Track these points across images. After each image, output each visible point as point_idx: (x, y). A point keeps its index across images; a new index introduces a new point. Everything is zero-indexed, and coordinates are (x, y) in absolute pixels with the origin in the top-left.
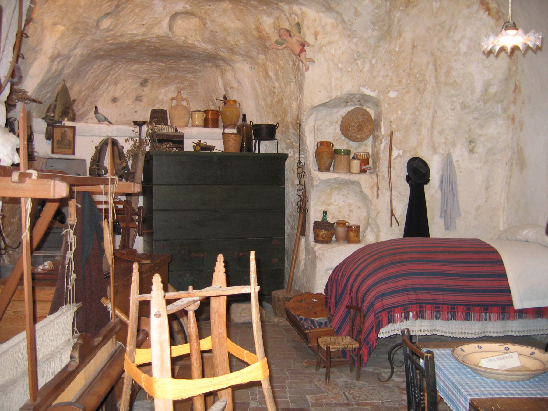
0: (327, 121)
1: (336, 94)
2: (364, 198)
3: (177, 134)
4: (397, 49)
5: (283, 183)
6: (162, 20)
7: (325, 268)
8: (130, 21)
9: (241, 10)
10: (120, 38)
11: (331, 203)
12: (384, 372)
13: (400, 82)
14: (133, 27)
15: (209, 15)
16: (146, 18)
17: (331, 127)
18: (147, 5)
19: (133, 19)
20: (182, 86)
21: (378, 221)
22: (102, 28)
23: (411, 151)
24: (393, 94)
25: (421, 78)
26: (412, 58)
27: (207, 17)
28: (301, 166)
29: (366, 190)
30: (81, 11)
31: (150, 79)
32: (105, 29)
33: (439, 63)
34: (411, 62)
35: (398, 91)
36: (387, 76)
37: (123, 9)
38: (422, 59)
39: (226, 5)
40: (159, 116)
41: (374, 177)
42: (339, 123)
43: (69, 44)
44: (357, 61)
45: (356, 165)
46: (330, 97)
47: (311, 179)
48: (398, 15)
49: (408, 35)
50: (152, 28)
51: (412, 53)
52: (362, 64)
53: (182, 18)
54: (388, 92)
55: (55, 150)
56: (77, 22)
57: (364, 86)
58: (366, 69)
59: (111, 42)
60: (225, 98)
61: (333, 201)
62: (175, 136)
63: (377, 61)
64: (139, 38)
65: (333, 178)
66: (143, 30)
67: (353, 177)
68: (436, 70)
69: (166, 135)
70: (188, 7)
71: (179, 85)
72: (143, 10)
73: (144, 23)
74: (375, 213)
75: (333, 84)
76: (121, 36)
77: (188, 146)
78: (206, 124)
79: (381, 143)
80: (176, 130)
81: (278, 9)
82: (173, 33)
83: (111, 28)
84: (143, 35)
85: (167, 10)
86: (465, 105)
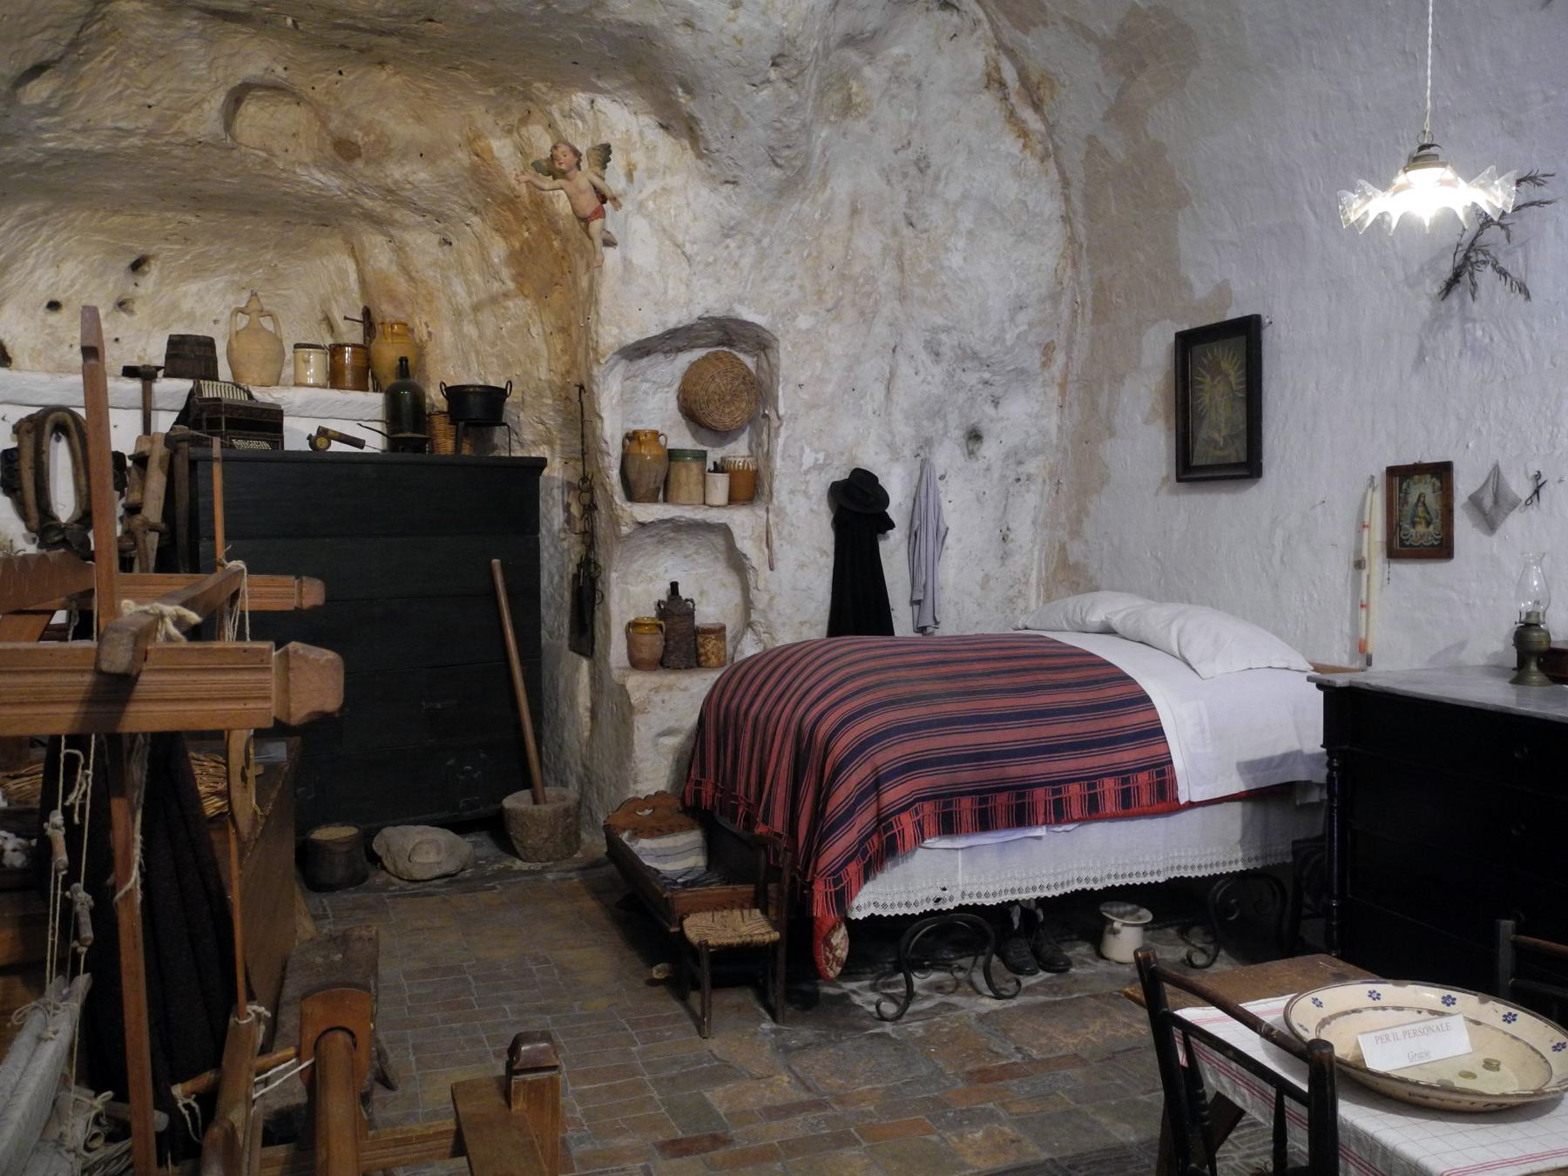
1: (676, 318)
2: (737, 563)
3: (251, 404)
4: (817, 216)
5: (535, 528)
6: (203, 100)
7: (655, 731)
8: (111, 93)
9: (426, 91)
11: (657, 575)
12: (854, 992)
13: (820, 293)
14: (120, 108)
15: (337, 99)
16: (158, 87)
17: (659, 395)
18: (162, 53)
19: (119, 88)
20: (246, 279)
21: (772, 616)
22: (25, 102)
23: (842, 454)
24: (804, 322)
25: (867, 288)
26: (850, 240)
27: (332, 103)
28: (586, 488)
29: (745, 545)
31: (154, 257)
32: (32, 107)
33: (909, 252)
34: (847, 248)
35: (816, 314)
36: (792, 278)
37: (89, 56)
38: (870, 243)
39: (384, 75)
41: (762, 513)
42: (676, 386)
44: (728, 241)
45: (720, 486)
46: (663, 324)
47: (615, 521)
48: (823, 134)
49: (841, 187)
50: (176, 117)
51: (851, 228)
52: (739, 247)
53: (259, 98)
54: (795, 318)
57: (741, 301)
58: (746, 262)
60: (367, 313)
61: (661, 570)
62: (246, 408)
63: (772, 242)
64: (136, 141)
65: (667, 516)
66: (148, 121)
67: (714, 516)
68: (901, 269)
70: (279, 70)
71: (236, 278)
72: (149, 64)
73: (151, 101)
74: (766, 597)
75: (671, 293)
77: (297, 435)
78: (335, 379)
79: (777, 435)
80: (250, 397)
81: (527, 97)
82: (233, 138)
83: (53, 105)
84: (149, 134)
85: (221, 73)
86: (964, 351)
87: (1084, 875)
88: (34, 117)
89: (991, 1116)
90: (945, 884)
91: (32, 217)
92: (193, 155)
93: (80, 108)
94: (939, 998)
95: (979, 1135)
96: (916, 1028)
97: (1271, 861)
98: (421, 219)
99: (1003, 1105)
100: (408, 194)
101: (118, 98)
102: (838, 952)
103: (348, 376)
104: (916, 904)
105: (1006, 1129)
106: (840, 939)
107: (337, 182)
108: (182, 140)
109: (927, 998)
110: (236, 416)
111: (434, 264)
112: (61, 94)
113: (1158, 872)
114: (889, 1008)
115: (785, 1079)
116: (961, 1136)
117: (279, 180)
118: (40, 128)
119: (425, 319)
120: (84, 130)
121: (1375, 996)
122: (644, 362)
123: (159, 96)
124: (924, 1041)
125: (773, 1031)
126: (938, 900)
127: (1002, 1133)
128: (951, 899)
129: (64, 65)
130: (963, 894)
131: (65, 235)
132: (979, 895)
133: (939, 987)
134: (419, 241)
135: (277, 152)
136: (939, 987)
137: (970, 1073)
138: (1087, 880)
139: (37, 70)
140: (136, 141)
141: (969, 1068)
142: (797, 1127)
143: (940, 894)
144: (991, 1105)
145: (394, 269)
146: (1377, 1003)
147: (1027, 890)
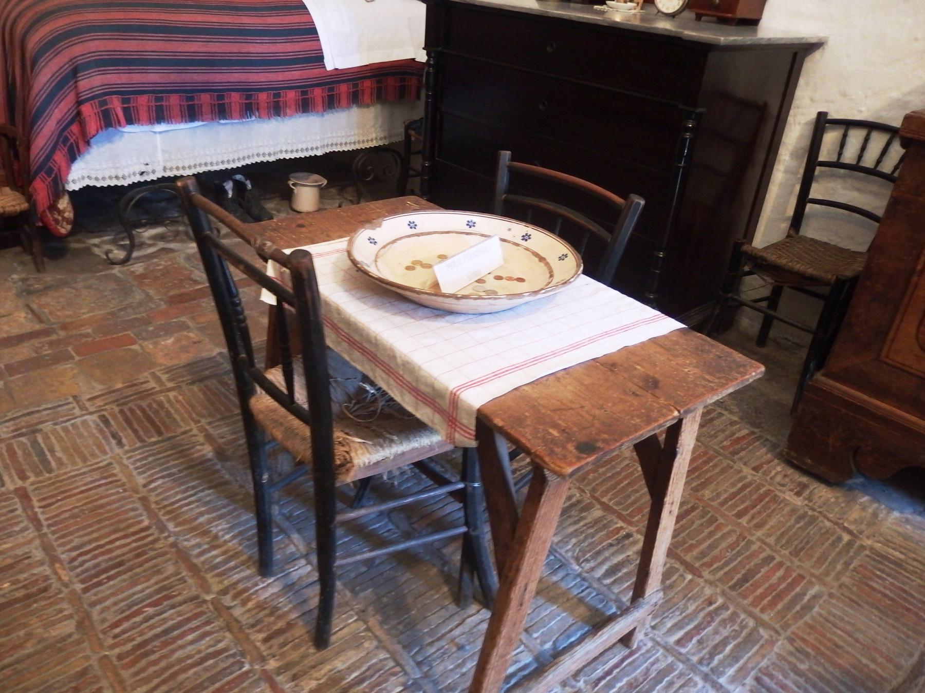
12: (95, 245)
87: (261, 152)
89: (183, 327)
90: (148, 161)
94: (161, 245)
95: (170, 341)
96: (138, 268)
97: (394, 140)
99: (193, 318)
102: (66, 215)
104: (124, 178)
105: (191, 335)
106: (64, 203)
109: (150, 245)
113: (317, 148)
114: (119, 254)
115: (22, 316)
116: (156, 344)
121: (412, 225)
124: (143, 276)
125: (23, 280)
126: (142, 173)
127: (188, 338)
128: (154, 172)
130: (165, 169)
132: (178, 168)
133: (161, 237)
136: (161, 237)
137: (172, 297)
138: (264, 155)
141: (172, 293)
142: (24, 351)
143: (144, 169)
144: (183, 319)
146: (413, 231)
147: (217, 164)
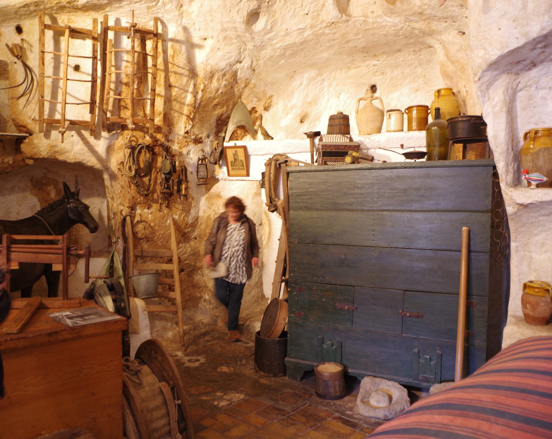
0: (543, 88)
8: (290, 14)
10: (287, 39)
14: (296, 20)
19: (292, 11)
22: (256, 30)
30: (219, 15)
32: (260, 32)
40: (340, 123)
43: (226, 57)
50: (318, 15)
55: (231, 173)
56: (224, 30)
59: (279, 45)
64: (308, 32)
66: (309, 21)
69: (335, 146)
73: (306, 12)
76: (287, 34)
84: (312, 27)
88: (264, 35)
91: (313, 79)
92: (335, 30)
93: (281, 26)
98: (445, 24)
100: (428, 11)
101: (294, 16)
103: (414, 125)
107: (398, 19)
108: (325, 25)
110: (328, 150)
111: (459, 50)
112: (270, 21)
117: (375, 28)
118: (269, 39)
119: (464, 84)
120: (287, 34)
122: (534, 72)
123: (307, 8)
129: (263, 9)
131: (334, 83)
134: (450, 38)
135: (370, 14)
139: (254, 16)
140: (308, 32)
145: (445, 58)
